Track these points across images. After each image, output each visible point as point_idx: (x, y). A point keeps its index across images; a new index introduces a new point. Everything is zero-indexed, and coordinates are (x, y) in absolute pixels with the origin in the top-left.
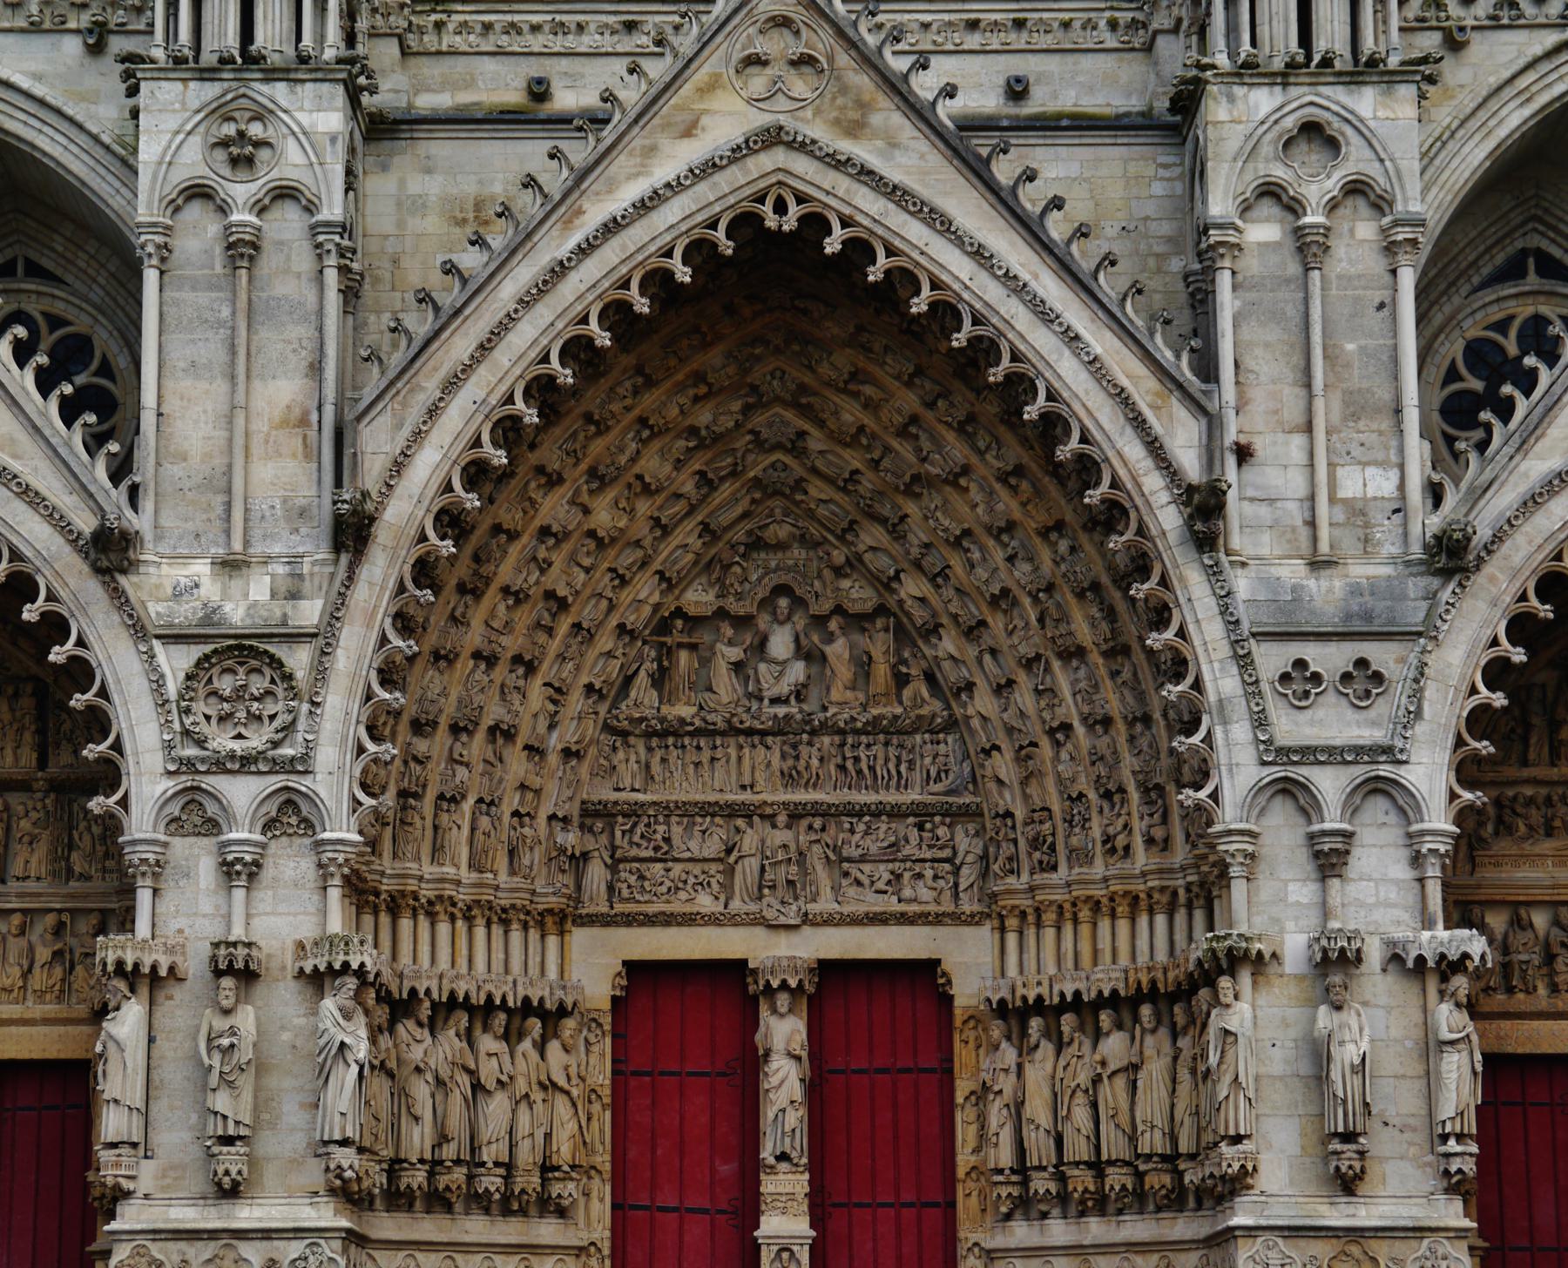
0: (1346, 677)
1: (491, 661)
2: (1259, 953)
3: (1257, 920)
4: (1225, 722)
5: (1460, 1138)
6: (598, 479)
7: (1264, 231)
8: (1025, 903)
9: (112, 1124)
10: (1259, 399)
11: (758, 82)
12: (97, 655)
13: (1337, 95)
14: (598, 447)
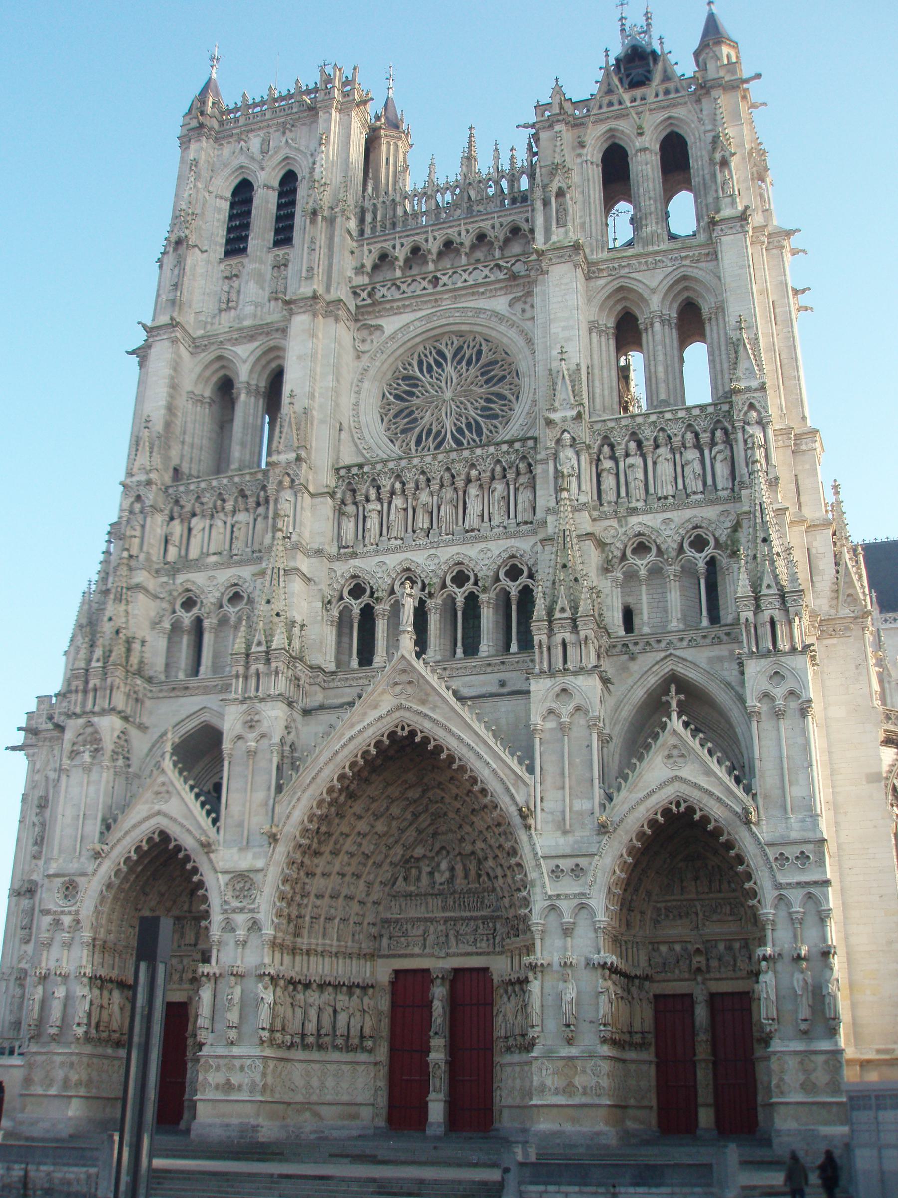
0: (572, 870)
1: (343, 875)
2: (542, 965)
3: (545, 953)
4: (533, 886)
5: (605, 1025)
6: (377, 817)
7: (551, 724)
8: (511, 947)
9: (200, 1022)
10: (549, 780)
11: (398, 689)
12: (205, 879)
13: (571, 678)
14: (374, 806)
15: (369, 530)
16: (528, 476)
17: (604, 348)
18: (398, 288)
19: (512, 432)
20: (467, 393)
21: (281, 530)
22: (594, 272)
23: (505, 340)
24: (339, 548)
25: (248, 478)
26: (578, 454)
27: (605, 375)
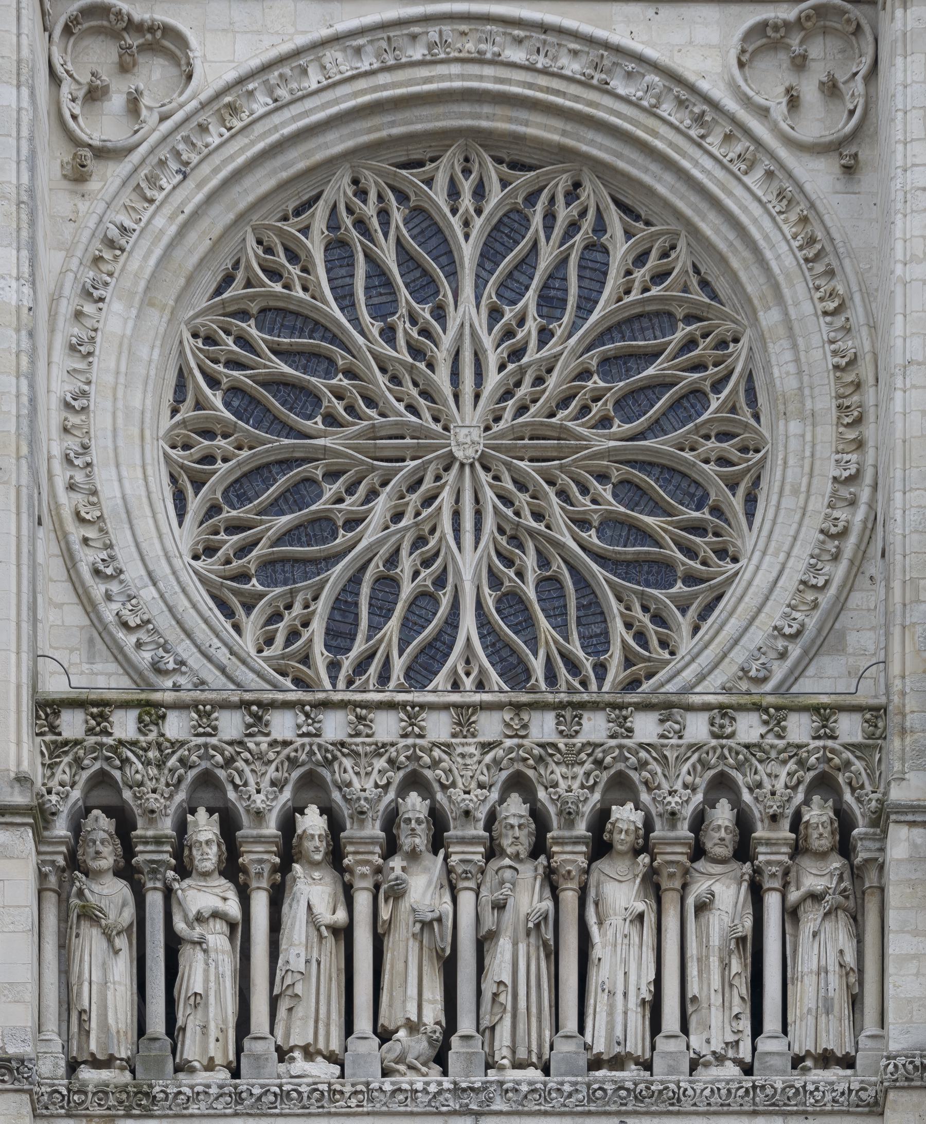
15: (198, 1000)
16: (836, 863)
24: (73, 1067)
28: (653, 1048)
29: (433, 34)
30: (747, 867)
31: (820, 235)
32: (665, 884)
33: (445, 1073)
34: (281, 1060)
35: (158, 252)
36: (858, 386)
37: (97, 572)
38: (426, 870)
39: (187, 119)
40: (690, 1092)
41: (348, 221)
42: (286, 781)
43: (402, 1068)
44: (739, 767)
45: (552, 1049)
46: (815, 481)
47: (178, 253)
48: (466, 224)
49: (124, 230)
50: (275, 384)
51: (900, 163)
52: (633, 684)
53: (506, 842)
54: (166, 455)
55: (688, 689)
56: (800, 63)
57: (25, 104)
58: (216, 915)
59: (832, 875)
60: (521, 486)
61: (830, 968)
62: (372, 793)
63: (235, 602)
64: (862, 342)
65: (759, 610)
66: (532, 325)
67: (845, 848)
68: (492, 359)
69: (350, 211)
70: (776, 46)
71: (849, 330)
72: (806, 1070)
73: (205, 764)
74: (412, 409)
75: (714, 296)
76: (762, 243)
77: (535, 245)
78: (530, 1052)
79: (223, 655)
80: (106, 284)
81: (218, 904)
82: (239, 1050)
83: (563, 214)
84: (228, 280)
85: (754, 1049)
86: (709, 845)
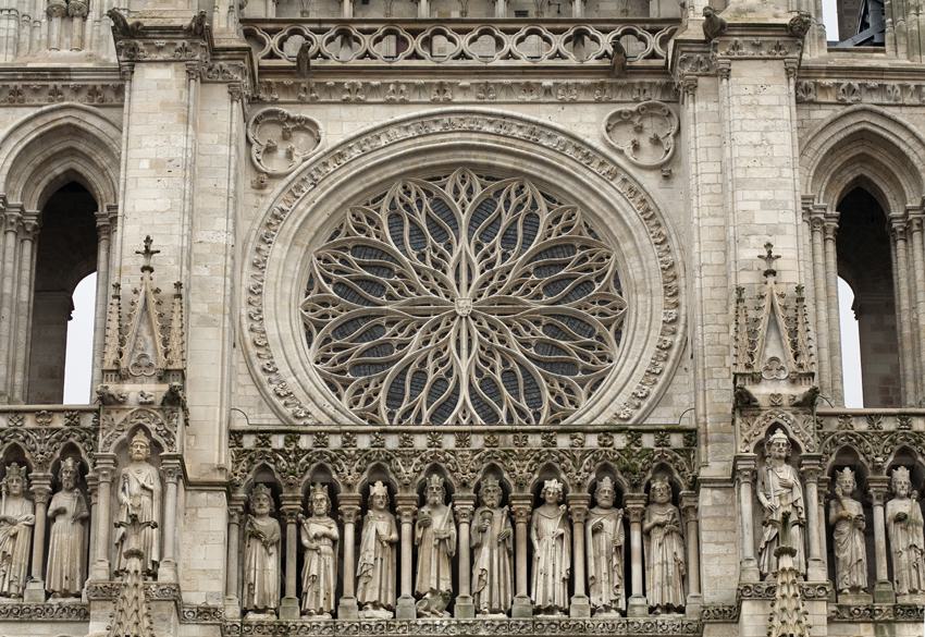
15: (315, 579)
16: (671, 508)
17: (820, 259)
18: (347, 38)
19: (614, 408)
20: (505, 306)
21: (137, 554)
22: (807, 90)
23: (593, 204)
24: (244, 612)
25: (30, 422)
26: (802, 477)
27: (823, 316)
28: (570, 603)
29: (446, 119)
30: (621, 511)
31: (652, 207)
32: (575, 519)
33: (452, 616)
34: (360, 609)
35: (300, 220)
36: (675, 277)
37: (264, 370)
38: (441, 513)
39: (317, 160)
40: (591, 625)
41: (401, 205)
42: (365, 470)
43: (428, 613)
44: (614, 461)
45: (512, 603)
46: (653, 324)
47: (311, 222)
48: (463, 206)
49: (282, 211)
50: (361, 280)
51: (694, 172)
52: (556, 421)
53: (485, 499)
54: (302, 314)
55: (588, 424)
56: (639, 130)
57: (233, 153)
58: (325, 536)
59: (669, 514)
60: (493, 327)
61: (669, 561)
62: (412, 475)
63: (338, 384)
64: (677, 256)
65: (624, 386)
66: (498, 252)
67: (676, 500)
68: (477, 268)
69: (401, 200)
70: (625, 122)
71: (669, 251)
72: (657, 614)
73: (320, 461)
74: (433, 291)
75: (596, 237)
76: (621, 212)
77: (500, 215)
78: (500, 605)
79: (331, 410)
80: (273, 236)
81: (325, 530)
82: (337, 604)
83: (514, 200)
84: (337, 233)
85: (627, 603)
86: (599, 500)
